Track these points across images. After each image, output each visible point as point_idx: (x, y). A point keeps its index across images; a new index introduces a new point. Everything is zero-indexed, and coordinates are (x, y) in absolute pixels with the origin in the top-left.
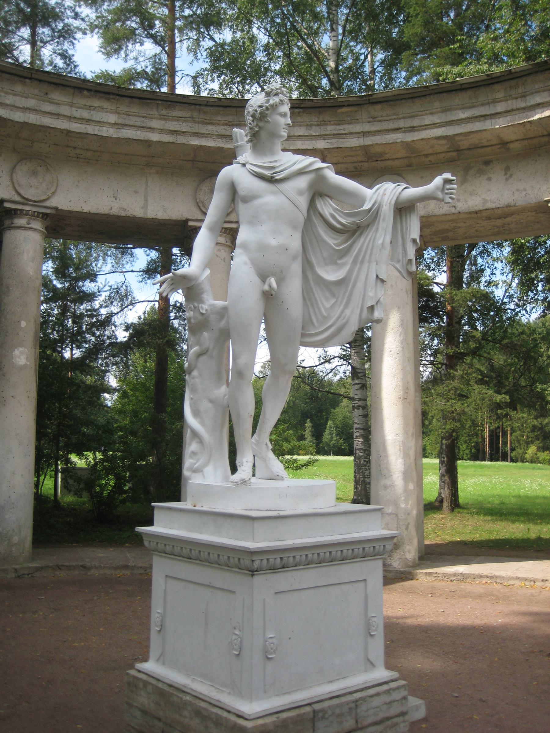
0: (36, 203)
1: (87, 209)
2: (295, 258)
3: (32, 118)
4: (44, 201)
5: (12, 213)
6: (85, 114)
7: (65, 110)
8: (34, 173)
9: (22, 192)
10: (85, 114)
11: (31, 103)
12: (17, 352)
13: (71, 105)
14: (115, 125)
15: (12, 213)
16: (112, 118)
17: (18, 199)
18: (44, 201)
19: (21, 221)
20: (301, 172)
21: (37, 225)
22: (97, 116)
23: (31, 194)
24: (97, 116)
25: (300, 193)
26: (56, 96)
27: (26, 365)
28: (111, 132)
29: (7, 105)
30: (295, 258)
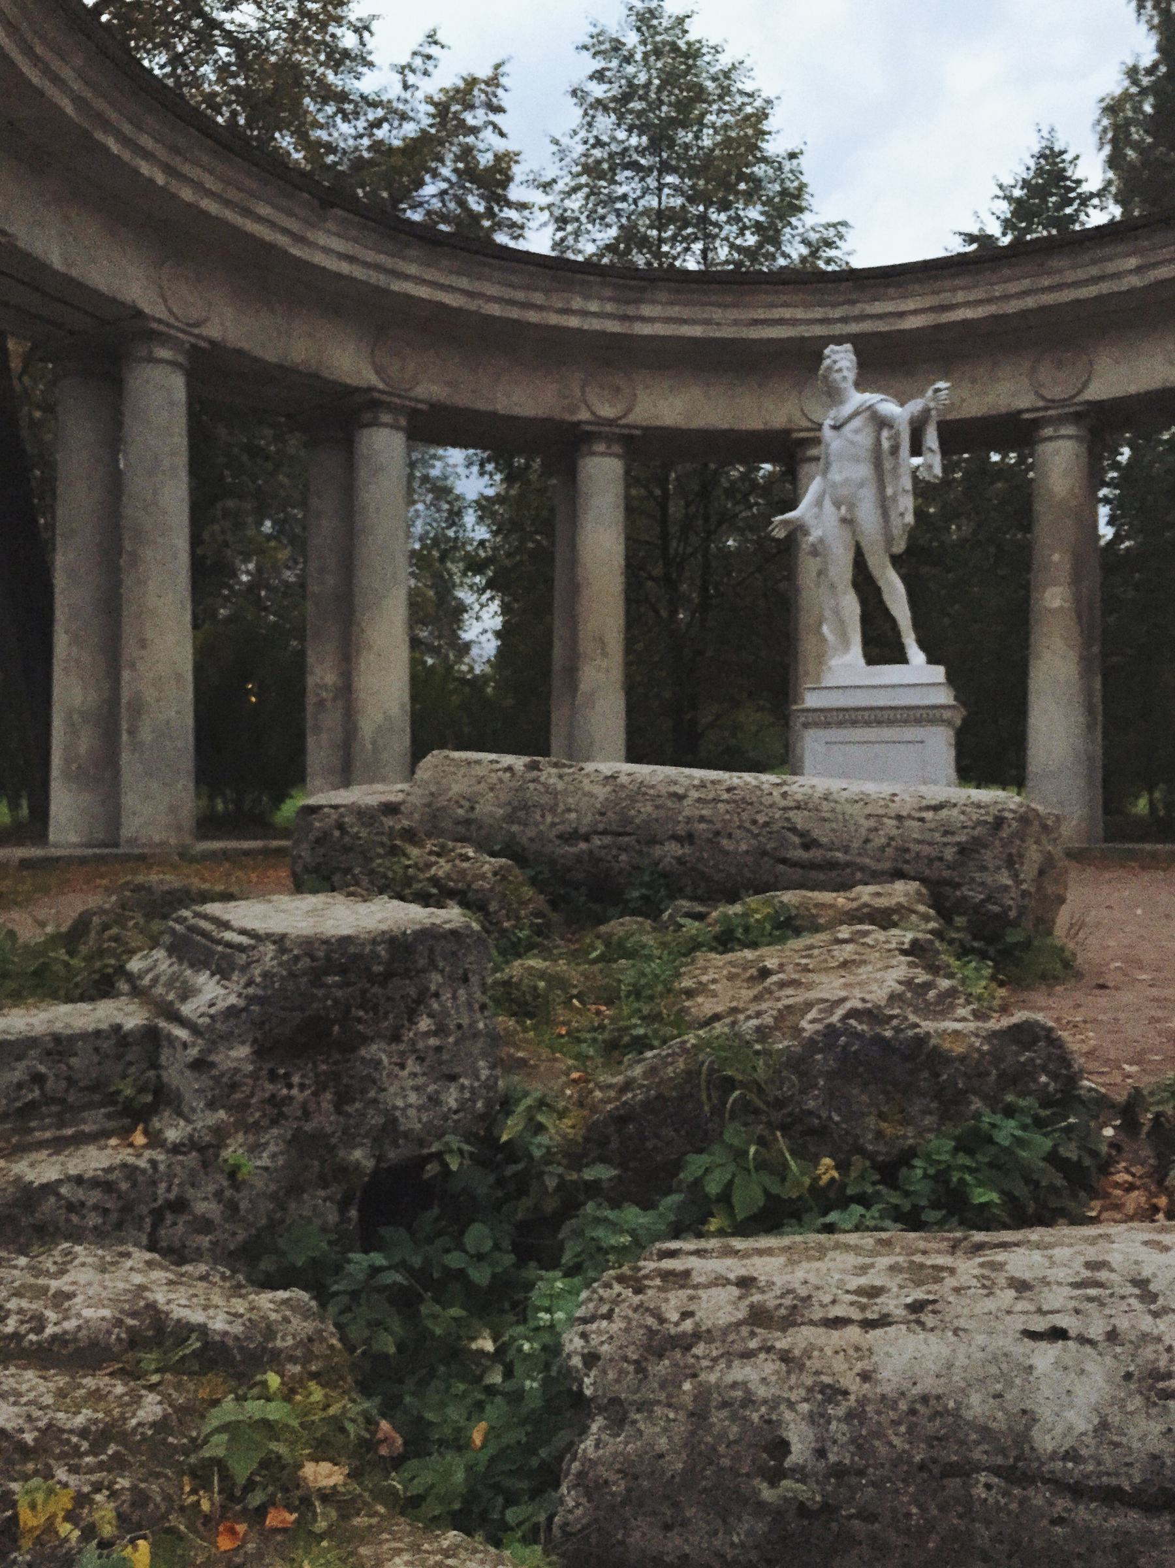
0: (1063, 402)
1: (1132, 389)
2: (861, 485)
3: (1030, 302)
4: (1074, 396)
5: (1036, 424)
6: (1094, 271)
7: (1070, 276)
8: (1059, 364)
9: (1045, 393)
10: (1094, 271)
11: (1026, 284)
12: (1047, 594)
13: (1074, 267)
14: (1139, 270)
15: (1036, 424)
16: (1133, 262)
17: (1041, 404)
18: (1074, 396)
19: (1048, 431)
20: (856, 414)
21: (1070, 430)
22: (1111, 267)
23: (1057, 392)
24: (1111, 267)
25: (856, 432)
26: (1055, 263)
27: (1061, 607)
28: (1135, 281)
29: (997, 298)
30: (861, 485)
